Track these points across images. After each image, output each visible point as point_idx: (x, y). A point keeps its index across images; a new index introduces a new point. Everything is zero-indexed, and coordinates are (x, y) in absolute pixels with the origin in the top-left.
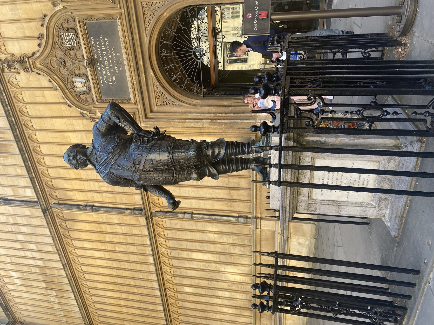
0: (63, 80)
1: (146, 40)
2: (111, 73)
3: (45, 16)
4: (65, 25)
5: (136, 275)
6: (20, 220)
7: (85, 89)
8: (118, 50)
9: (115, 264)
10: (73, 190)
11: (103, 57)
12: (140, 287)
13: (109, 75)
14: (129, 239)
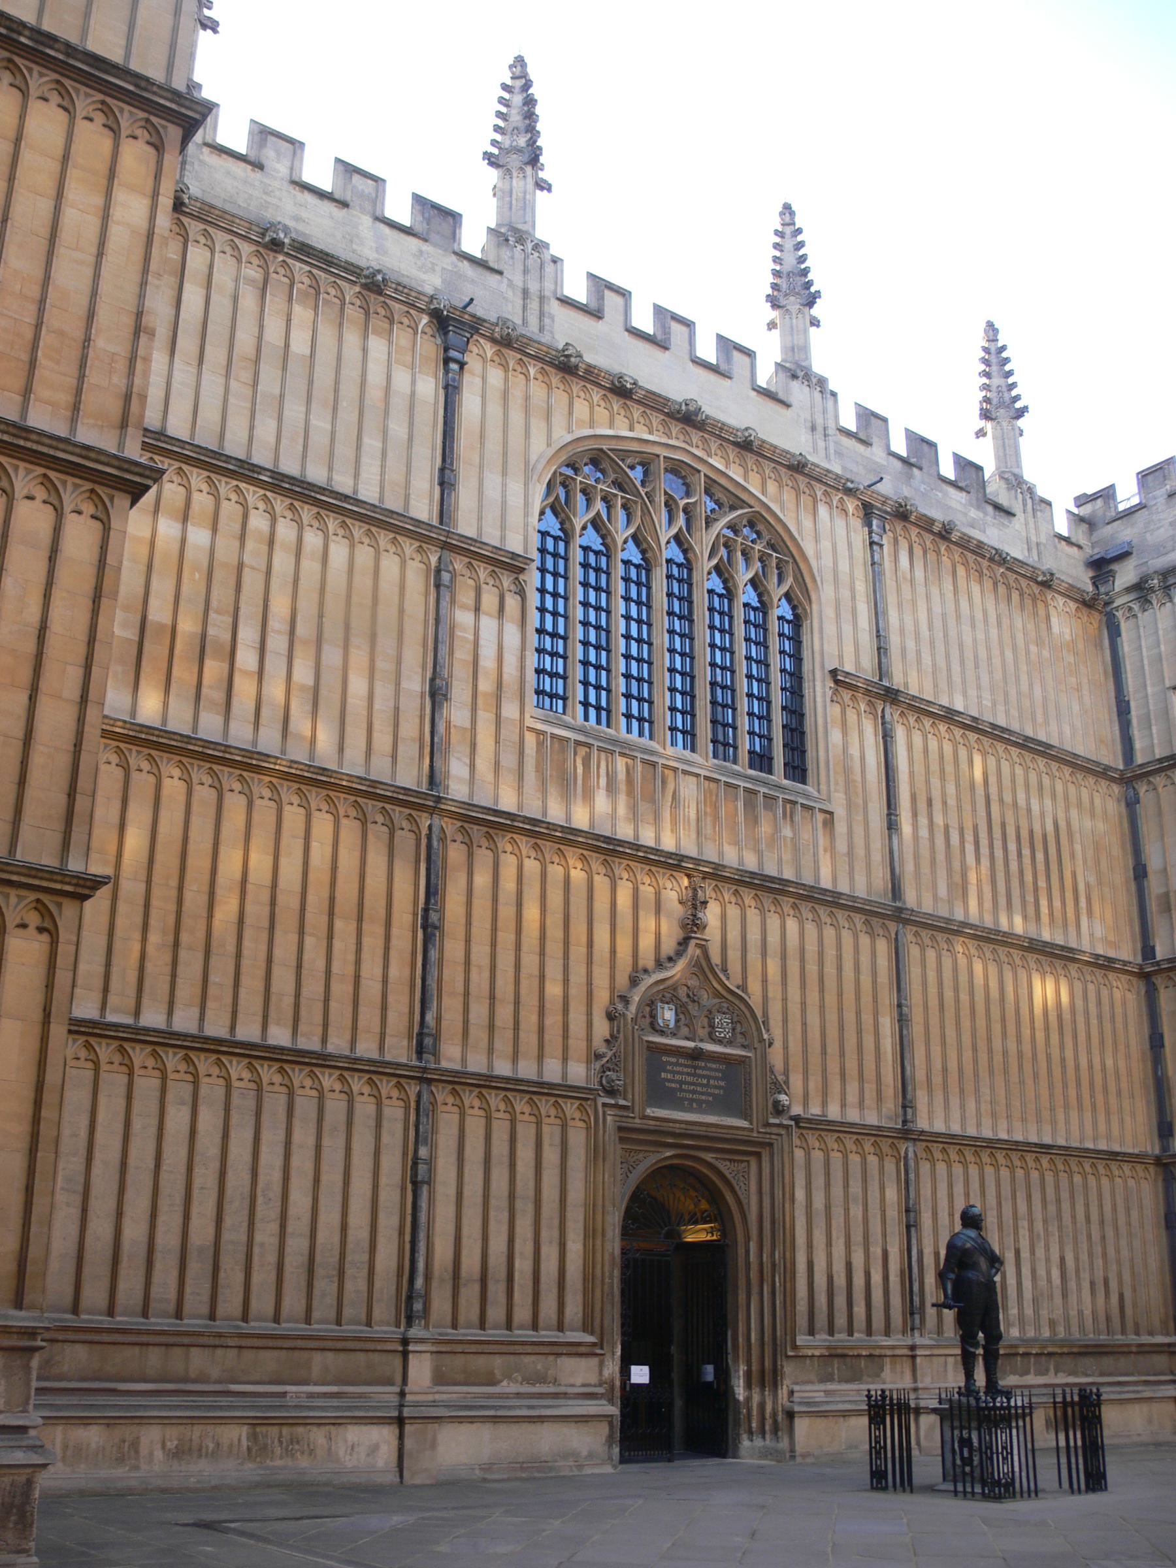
1: (709, 1157)
2: (681, 1083)
4: (738, 1029)
7: (660, 1021)
8: (711, 1108)
13: (677, 1077)
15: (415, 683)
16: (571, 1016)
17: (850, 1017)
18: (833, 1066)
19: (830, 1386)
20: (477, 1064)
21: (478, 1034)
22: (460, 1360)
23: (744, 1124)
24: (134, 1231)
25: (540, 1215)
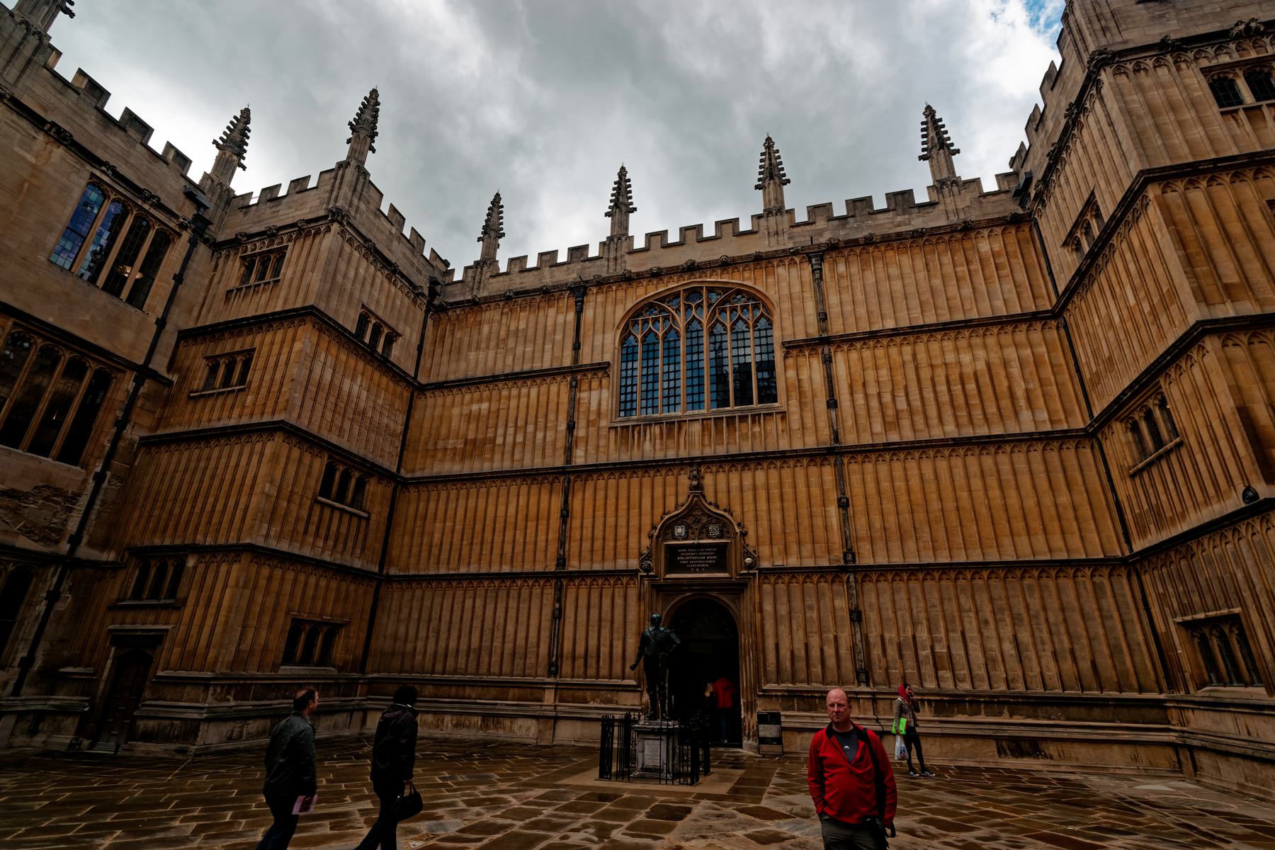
0: (685, 517)
1: (714, 594)
6: (550, 434)
8: (707, 570)
9: (499, 526)
10: (583, 500)
14: (530, 547)
15: (563, 427)
16: (631, 539)
17: (804, 512)
18: (792, 538)
20: (585, 567)
21: (586, 554)
22: (570, 692)
23: (726, 575)
24: (453, 645)
25: (615, 627)
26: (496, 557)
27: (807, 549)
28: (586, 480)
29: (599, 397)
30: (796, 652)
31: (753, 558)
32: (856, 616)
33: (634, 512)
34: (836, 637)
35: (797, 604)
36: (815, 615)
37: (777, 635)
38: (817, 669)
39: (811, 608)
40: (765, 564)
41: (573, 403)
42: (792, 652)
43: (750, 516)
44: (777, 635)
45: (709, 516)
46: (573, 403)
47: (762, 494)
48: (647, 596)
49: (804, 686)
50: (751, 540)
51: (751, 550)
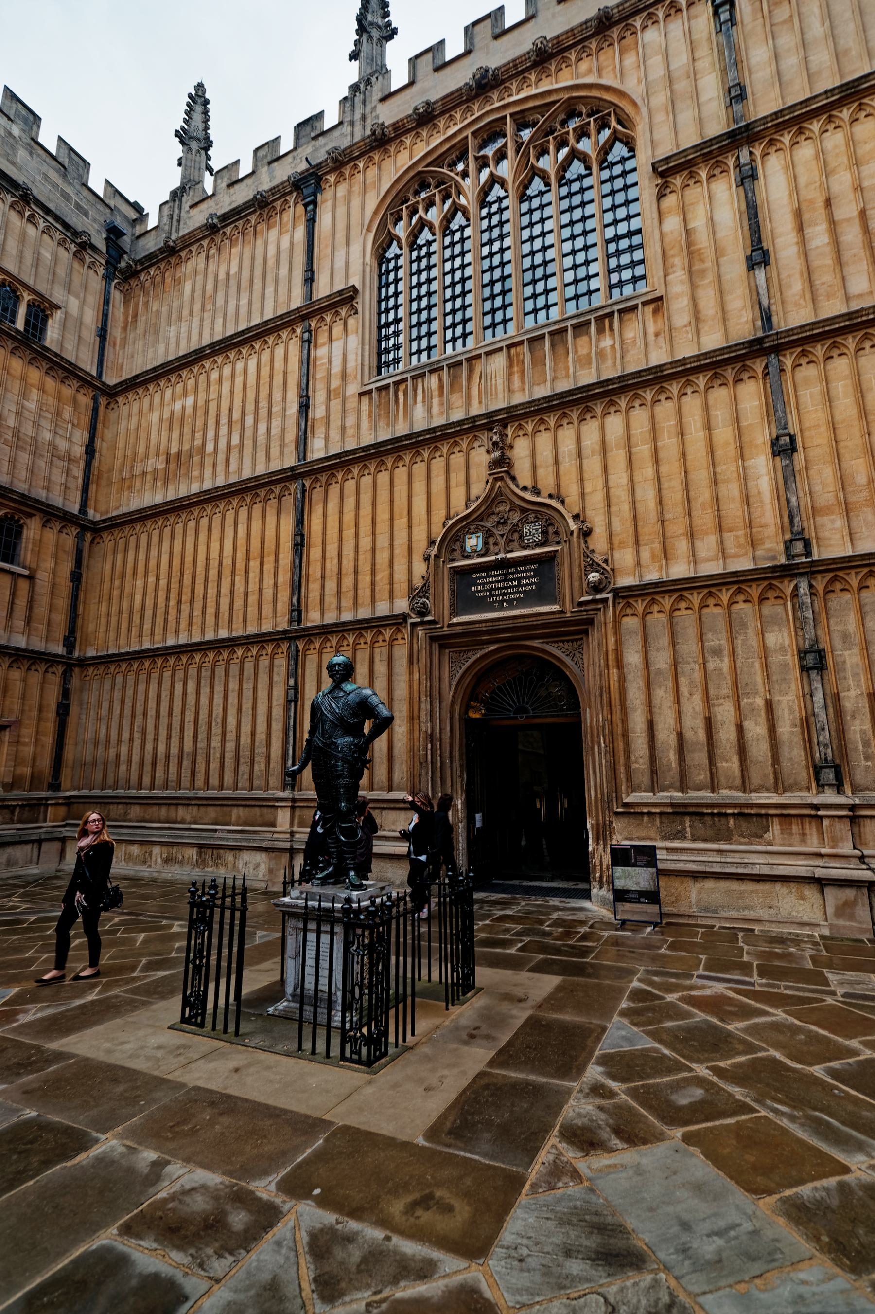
0: (480, 518)
1: (536, 643)
3: (563, 502)
4: (551, 530)
5: (198, 605)
6: (276, 423)
7: (468, 550)
8: (521, 603)
9: (213, 573)
10: (325, 515)
11: (511, 580)
12: (179, 611)
13: (487, 587)
14: (253, 599)
15: (293, 409)
16: (396, 567)
17: (701, 476)
18: (677, 528)
19: (676, 844)
20: (331, 618)
21: (331, 600)
24: (161, 748)
26: (210, 619)
27: (707, 545)
28: (328, 484)
29: (345, 348)
30: (688, 734)
31: (602, 572)
32: (814, 660)
33: (401, 523)
34: (769, 705)
35: (689, 647)
36: (725, 664)
37: (650, 705)
38: (730, 765)
39: (717, 652)
40: (625, 581)
41: (307, 365)
42: (680, 736)
43: (596, 500)
44: (650, 705)
45: (523, 510)
46: (307, 365)
47: (618, 458)
48: (423, 656)
49: (705, 795)
50: (599, 542)
51: (598, 558)
